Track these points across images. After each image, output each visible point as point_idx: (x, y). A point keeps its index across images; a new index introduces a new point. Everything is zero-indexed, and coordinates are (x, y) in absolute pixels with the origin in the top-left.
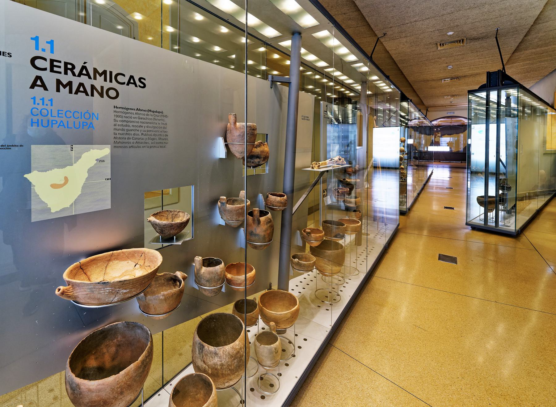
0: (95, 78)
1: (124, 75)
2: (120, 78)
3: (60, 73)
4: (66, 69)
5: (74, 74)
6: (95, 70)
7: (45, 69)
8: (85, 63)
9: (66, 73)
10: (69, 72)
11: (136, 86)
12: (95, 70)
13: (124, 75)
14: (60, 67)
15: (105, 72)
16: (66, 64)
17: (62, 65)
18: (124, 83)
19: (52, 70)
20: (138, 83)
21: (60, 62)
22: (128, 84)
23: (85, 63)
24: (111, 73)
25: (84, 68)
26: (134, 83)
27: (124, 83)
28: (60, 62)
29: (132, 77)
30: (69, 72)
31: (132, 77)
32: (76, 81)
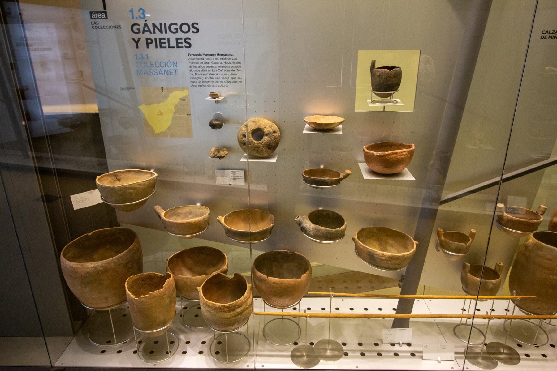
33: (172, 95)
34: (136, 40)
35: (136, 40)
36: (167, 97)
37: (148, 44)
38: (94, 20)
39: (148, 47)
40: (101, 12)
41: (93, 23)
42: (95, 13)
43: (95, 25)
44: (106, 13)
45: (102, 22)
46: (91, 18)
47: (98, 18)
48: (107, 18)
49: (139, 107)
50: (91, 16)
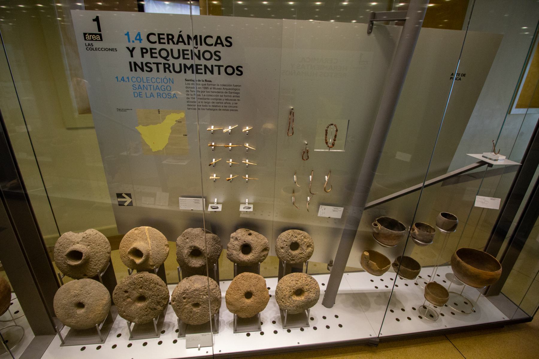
0: (189, 44)
1: (211, 37)
2: (209, 41)
3: (164, 43)
4: (168, 39)
5: (174, 43)
6: (189, 37)
7: (155, 42)
8: (180, 32)
9: (168, 43)
10: (170, 41)
11: (223, 46)
12: (189, 37)
13: (211, 37)
14: (164, 39)
15: (196, 37)
16: (168, 35)
17: (165, 37)
18: (212, 45)
19: (160, 43)
20: (225, 43)
21: (163, 34)
22: (215, 45)
23: (180, 32)
24: (201, 36)
25: (180, 36)
26: (221, 43)
27: (212, 45)
28: (163, 34)
29: (219, 38)
30: (170, 41)
31: (219, 38)
32: (175, 48)
33: (168, 117)
34: (131, 49)
35: (131, 49)
36: (164, 119)
37: (143, 53)
38: (87, 42)
39: (143, 57)
40: (96, 34)
41: (87, 45)
42: (90, 34)
43: (89, 47)
44: (100, 35)
45: (96, 44)
46: (85, 40)
47: (92, 40)
48: (102, 40)
49: (140, 129)
50: (85, 37)
